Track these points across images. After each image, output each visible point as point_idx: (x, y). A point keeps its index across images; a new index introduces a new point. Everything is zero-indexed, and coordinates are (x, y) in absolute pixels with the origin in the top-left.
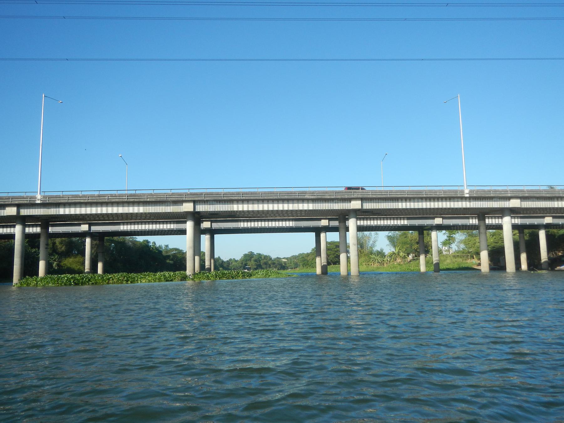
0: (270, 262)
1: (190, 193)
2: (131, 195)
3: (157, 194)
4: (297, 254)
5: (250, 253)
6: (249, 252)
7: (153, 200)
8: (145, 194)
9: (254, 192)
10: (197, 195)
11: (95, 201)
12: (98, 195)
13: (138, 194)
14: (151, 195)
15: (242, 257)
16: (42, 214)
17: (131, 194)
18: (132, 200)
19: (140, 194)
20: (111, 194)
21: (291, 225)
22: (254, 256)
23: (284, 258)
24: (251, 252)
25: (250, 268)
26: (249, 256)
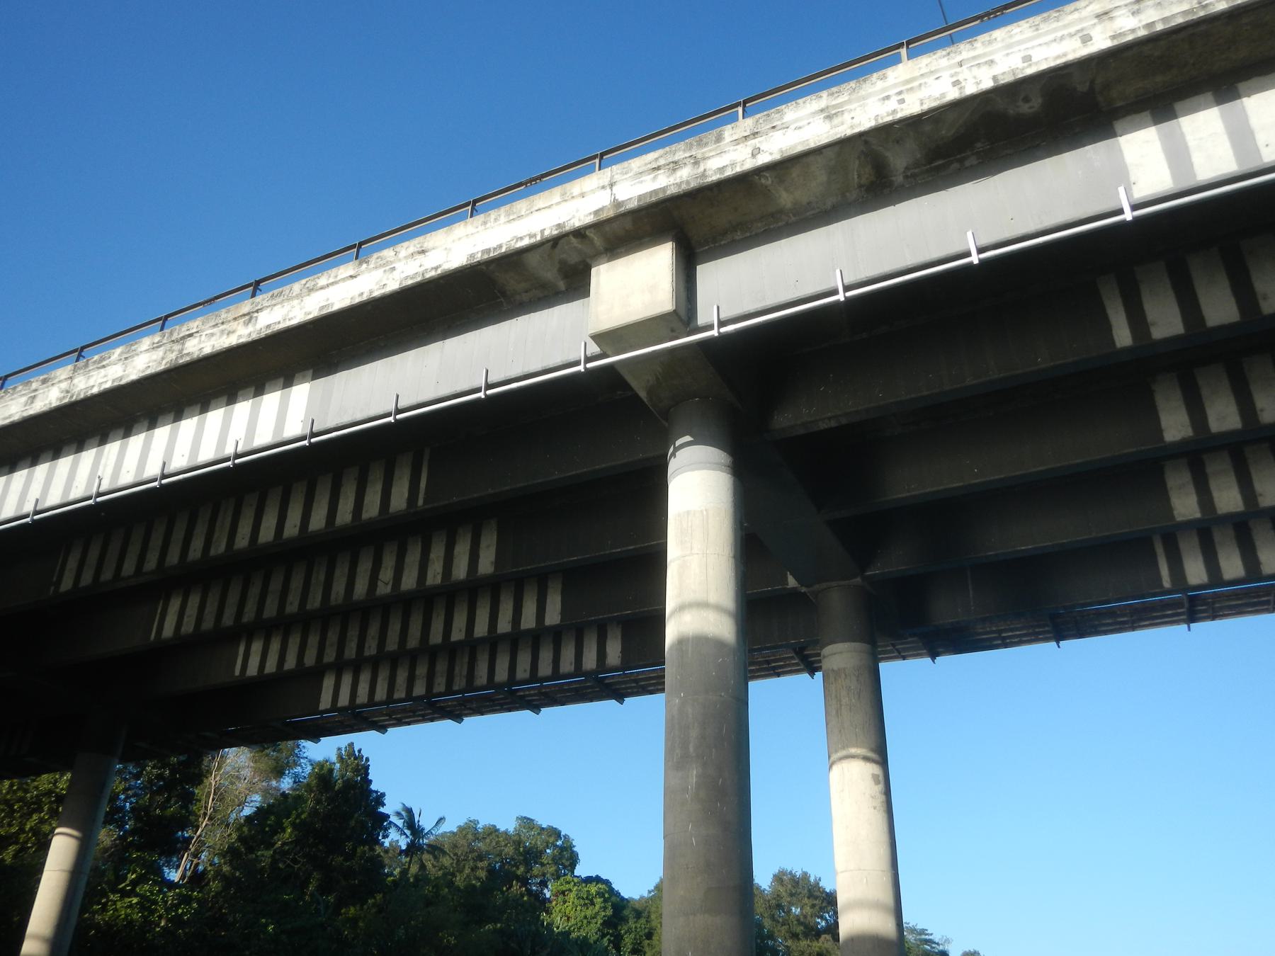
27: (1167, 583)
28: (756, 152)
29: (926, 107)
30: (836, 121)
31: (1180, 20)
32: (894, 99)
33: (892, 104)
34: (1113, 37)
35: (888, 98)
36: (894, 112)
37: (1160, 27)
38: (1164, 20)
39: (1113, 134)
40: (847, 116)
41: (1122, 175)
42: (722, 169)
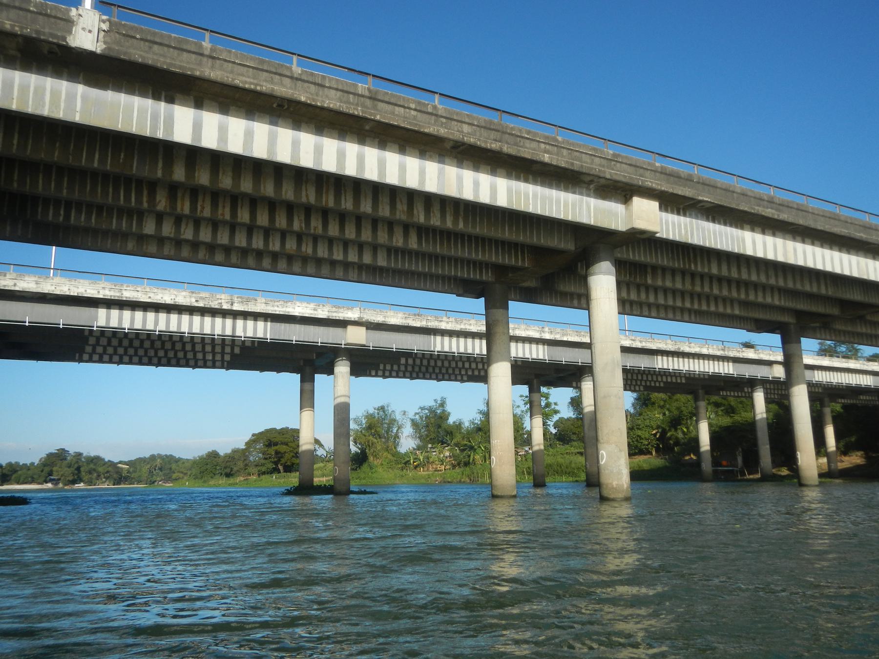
0: (101, 469)
1: (662, 167)
2: (488, 127)
3: (573, 144)
4: (147, 456)
5: (61, 451)
6: (58, 450)
7: (562, 161)
8: (535, 134)
9: (802, 205)
10: (679, 177)
11: (358, 111)
12: (369, 89)
13: (512, 129)
14: (551, 142)
15: (41, 459)
16: (77, 118)
17: (491, 122)
18: (495, 146)
19: (520, 131)
20: (419, 103)
21: (541, 357)
22: (69, 458)
23: (120, 462)
24: (63, 449)
25: (59, 479)
26: (59, 457)
27: (77, 358)
28: (15, 285)
29: (61, 293)
30: (38, 285)
31: (116, 298)
32: (54, 286)
33: (53, 288)
34: (104, 295)
35: (52, 285)
36: (53, 291)
37: (113, 298)
38: (114, 296)
39: (97, 307)
40: (41, 286)
41: (96, 319)
42: (5, 286)
